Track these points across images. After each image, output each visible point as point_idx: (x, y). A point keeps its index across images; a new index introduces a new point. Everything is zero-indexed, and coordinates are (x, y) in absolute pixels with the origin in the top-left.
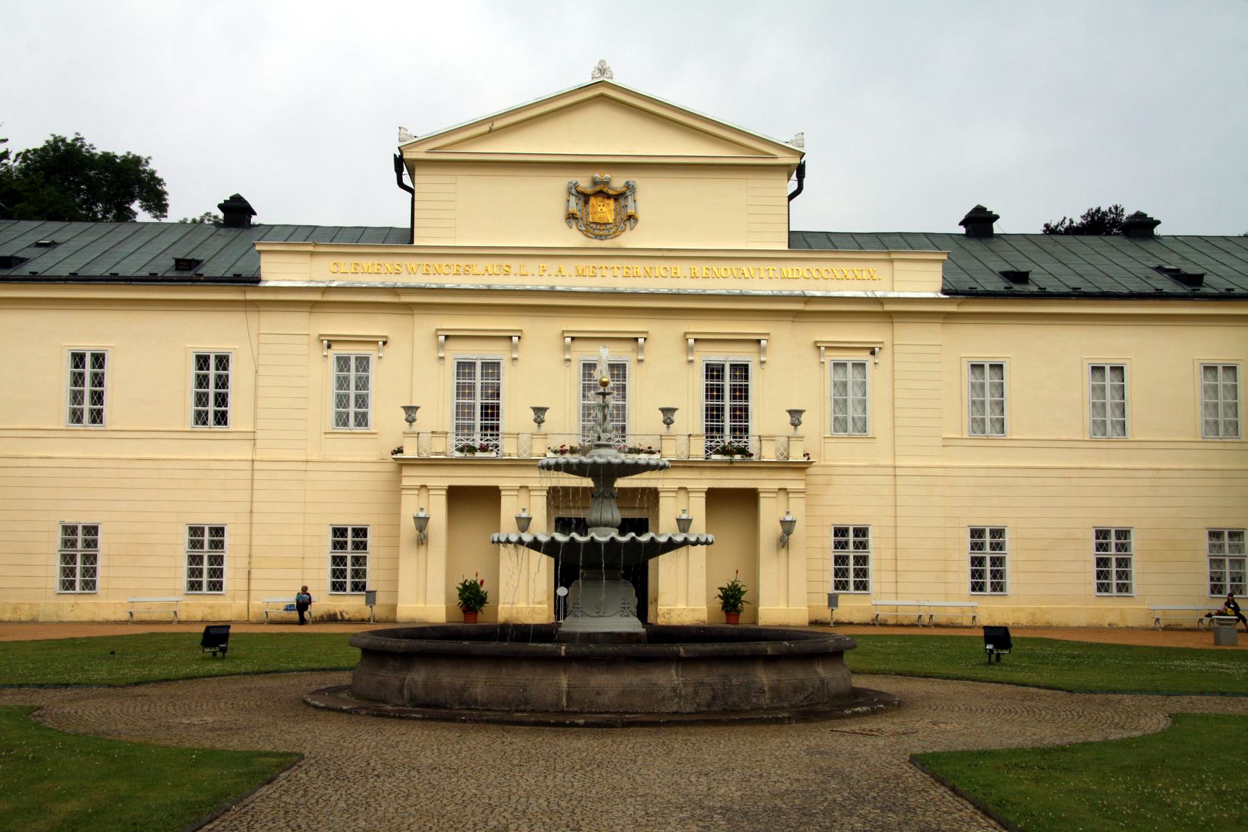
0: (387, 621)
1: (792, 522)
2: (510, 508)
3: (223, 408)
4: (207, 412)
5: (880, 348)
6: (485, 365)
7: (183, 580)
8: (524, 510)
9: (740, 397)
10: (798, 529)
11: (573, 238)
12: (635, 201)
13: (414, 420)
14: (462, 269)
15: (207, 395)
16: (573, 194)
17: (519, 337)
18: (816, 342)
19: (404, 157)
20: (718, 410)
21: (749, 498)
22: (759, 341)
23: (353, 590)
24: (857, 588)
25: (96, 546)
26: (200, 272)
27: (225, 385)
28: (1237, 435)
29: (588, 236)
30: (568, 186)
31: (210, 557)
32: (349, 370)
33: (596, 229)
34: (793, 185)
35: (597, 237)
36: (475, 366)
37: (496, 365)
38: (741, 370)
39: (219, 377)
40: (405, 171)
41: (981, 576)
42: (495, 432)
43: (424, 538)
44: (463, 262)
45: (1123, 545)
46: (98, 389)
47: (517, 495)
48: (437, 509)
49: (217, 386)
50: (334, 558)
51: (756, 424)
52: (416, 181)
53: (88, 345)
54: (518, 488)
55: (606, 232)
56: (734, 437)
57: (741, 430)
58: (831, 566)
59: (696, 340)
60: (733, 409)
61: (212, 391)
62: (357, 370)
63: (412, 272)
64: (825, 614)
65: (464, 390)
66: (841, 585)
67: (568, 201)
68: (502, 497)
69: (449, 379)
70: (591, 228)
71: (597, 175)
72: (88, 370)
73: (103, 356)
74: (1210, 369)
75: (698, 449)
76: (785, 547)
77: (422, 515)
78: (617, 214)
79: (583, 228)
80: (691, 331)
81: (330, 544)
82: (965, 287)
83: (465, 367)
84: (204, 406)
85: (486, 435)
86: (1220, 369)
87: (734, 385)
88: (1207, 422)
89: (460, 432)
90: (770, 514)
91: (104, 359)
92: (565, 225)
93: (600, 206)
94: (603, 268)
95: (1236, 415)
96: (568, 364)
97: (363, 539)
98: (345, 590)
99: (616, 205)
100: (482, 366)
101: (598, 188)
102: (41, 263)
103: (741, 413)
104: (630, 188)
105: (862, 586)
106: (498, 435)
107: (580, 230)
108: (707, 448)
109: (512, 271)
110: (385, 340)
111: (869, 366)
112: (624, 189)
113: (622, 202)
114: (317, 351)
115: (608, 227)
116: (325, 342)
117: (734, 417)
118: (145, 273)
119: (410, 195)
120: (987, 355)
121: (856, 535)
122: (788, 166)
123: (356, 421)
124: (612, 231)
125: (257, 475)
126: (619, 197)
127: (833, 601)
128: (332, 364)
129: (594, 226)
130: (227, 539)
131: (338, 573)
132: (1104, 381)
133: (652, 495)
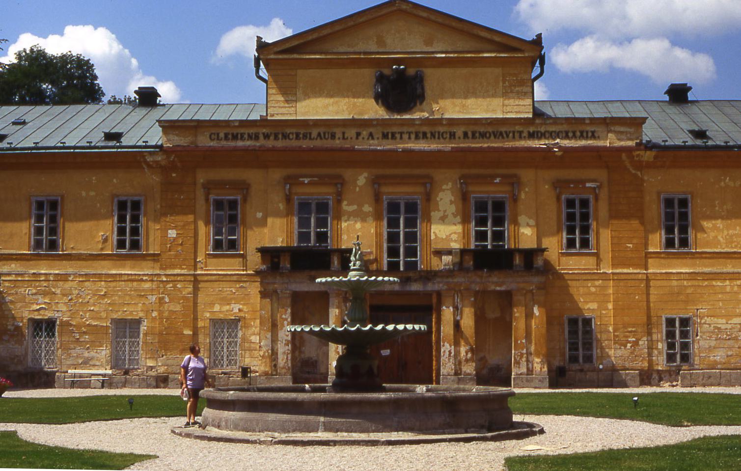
14: (301, 136)
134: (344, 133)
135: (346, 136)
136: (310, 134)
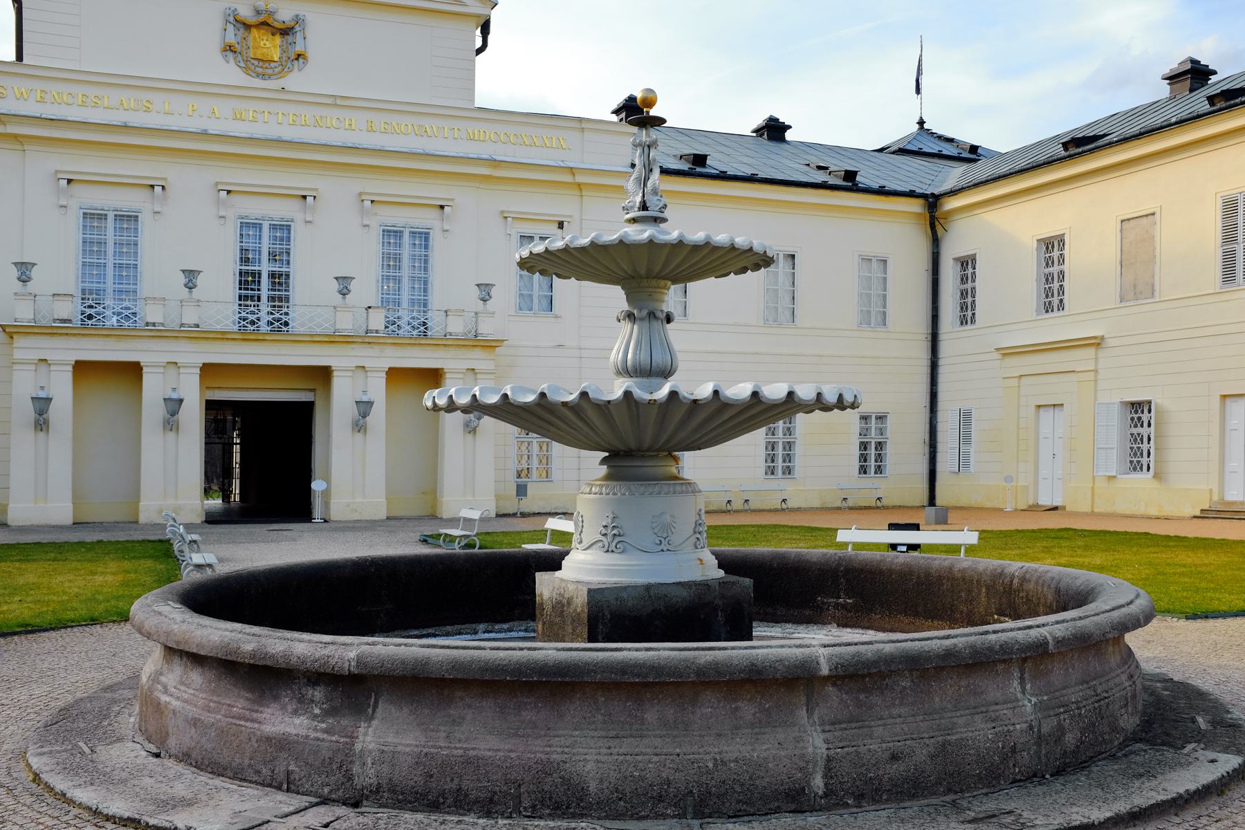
0: (115, 525)
5: (569, 222)
7: (761, 465)
8: (174, 389)
11: (231, 74)
12: (304, 38)
16: (230, 23)
17: (163, 187)
18: (502, 212)
22: (442, 207)
29: (248, 74)
30: (225, 13)
33: (259, 66)
36: (106, 219)
38: (423, 238)
43: (44, 423)
44: (92, 92)
47: (163, 373)
48: (61, 387)
54: (164, 364)
55: (269, 71)
67: (225, 30)
68: (145, 377)
69: (71, 232)
70: (253, 64)
76: (361, 431)
77: (42, 394)
79: (242, 64)
80: (367, 190)
86: (874, 260)
92: (219, 58)
93: (263, 40)
94: (266, 113)
96: (222, 221)
99: (283, 41)
101: (261, 18)
107: (240, 67)
108: (388, 322)
112: (293, 24)
115: (273, 65)
122: (478, 16)
124: (277, 70)
126: (286, 32)
132: (778, 268)
133: (323, 375)
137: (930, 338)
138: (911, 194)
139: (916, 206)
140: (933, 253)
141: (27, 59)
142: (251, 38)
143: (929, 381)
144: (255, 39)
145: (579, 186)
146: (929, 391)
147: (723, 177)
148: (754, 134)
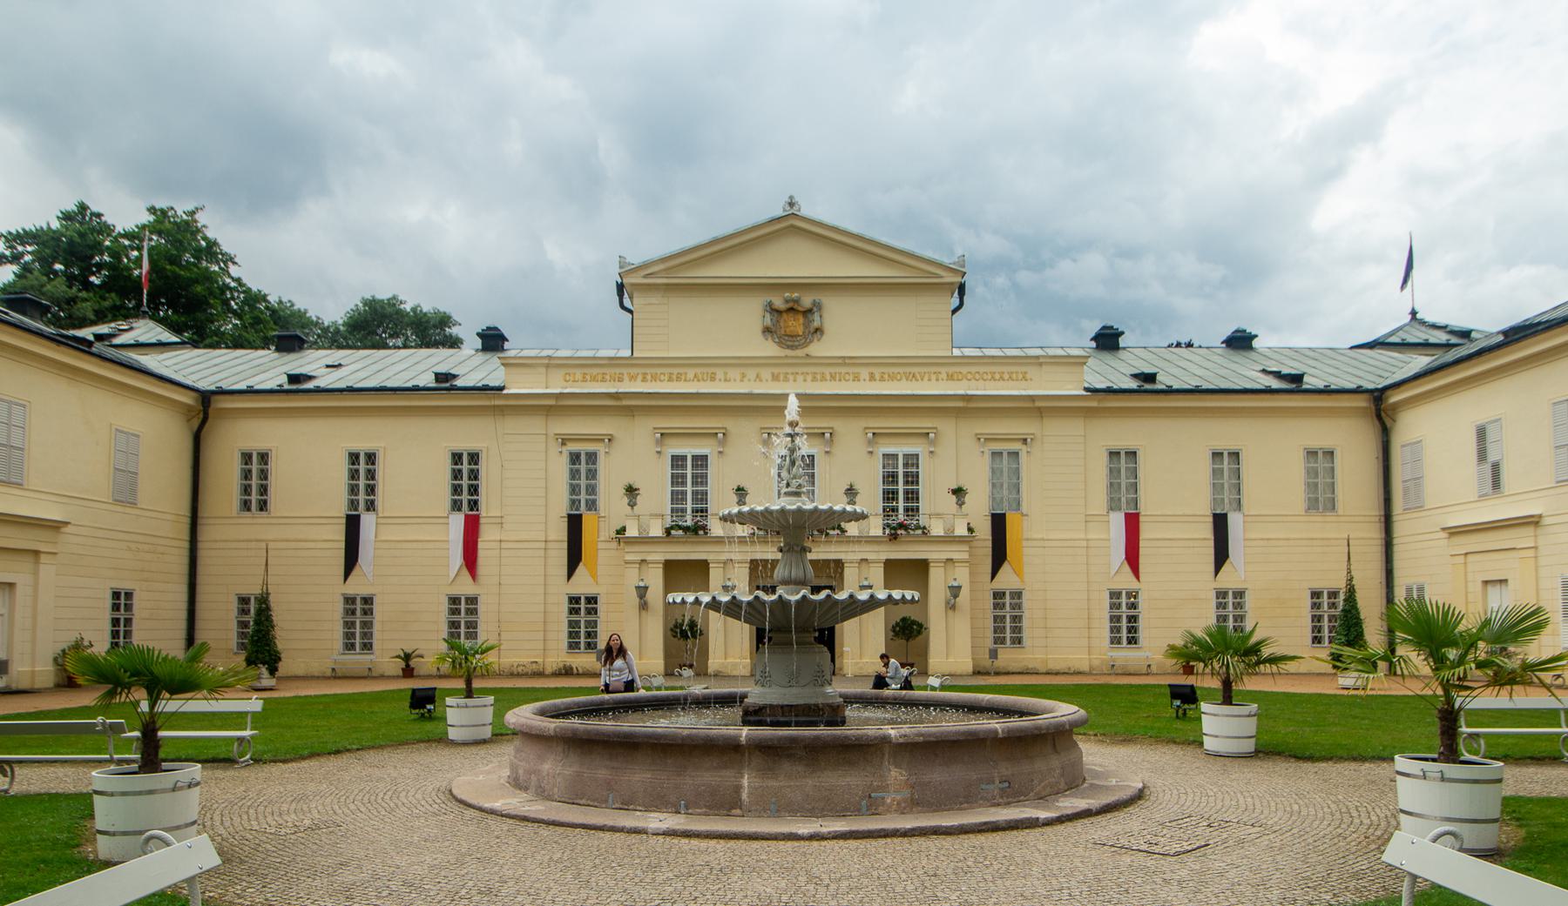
1: (959, 587)
2: (715, 576)
3: (475, 497)
4: (462, 500)
5: (1032, 439)
6: (695, 458)
9: (912, 483)
10: (965, 593)
11: (770, 349)
12: (821, 317)
13: (635, 504)
14: (674, 377)
15: (460, 486)
17: (724, 434)
18: (977, 434)
19: (625, 281)
20: (893, 493)
21: (922, 567)
23: (586, 649)
24: (1013, 643)
25: (372, 614)
26: (455, 383)
27: (476, 478)
28: (1334, 508)
31: (466, 622)
32: (580, 464)
33: (788, 340)
34: (955, 301)
35: (789, 347)
37: (704, 458)
39: (472, 471)
40: (626, 295)
41: (1119, 632)
42: (704, 514)
45: (1239, 603)
46: (372, 482)
48: (655, 579)
49: (470, 479)
50: (569, 621)
51: (924, 505)
52: (634, 302)
53: (362, 446)
55: (797, 343)
56: (907, 516)
57: (912, 510)
58: (990, 624)
59: (874, 434)
60: (906, 492)
61: (465, 482)
62: (587, 464)
63: (633, 378)
64: (986, 662)
65: (677, 480)
66: (1000, 641)
71: (787, 294)
72: (362, 467)
73: (374, 454)
74: (1311, 453)
75: (875, 527)
77: (642, 584)
78: (806, 326)
79: (777, 340)
81: (566, 610)
82: (1103, 386)
83: (678, 461)
84: (459, 495)
85: (696, 516)
86: (1320, 455)
87: (907, 472)
88: (1309, 499)
89: (674, 514)
90: (938, 580)
91: (375, 457)
95: (1333, 492)
97: (595, 606)
98: (580, 649)
100: (693, 460)
102: (326, 380)
103: (912, 496)
104: (817, 306)
105: (1018, 641)
106: (706, 516)
109: (718, 377)
110: (609, 437)
111: (1023, 456)
112: (811, 306)
113: (809, 315)
114: (554, 448)
115: (798, 339)
116: (560, 440)
117: (907, 499)
118: (409, 385)
119: (631, 316)
120: (1123, 442)
121: (1012, 598)
122: (952, 284)
123: (587, 506)
125: (504, 553)
126: (808, 312)
127: (994, 654)
128: (565, 459)
129: (786, 338)
130: (481, 607)
131: (573, 634)
134: (726, 374)
135: (728, 376)
136: (686, 374)
137: (1383, 519)
138: (1358, 391)
139: (1361, 402)
140: (1383, 442)
141: (635, 355)
142: (782, 321)
143: (1384, 558)
144: (785, 320)
145: (1039, 409)
146: (1384, 568)
147: (1170, 391)
148: (1224, 345)
